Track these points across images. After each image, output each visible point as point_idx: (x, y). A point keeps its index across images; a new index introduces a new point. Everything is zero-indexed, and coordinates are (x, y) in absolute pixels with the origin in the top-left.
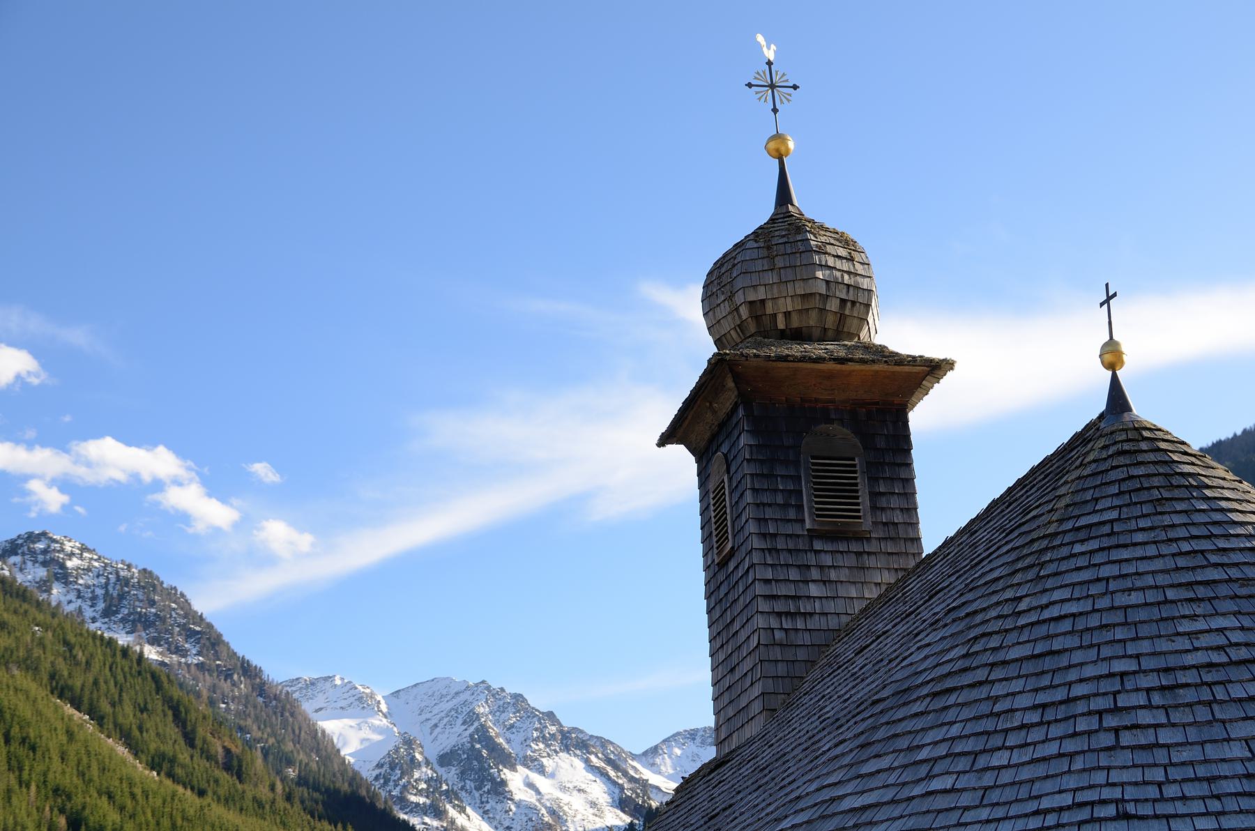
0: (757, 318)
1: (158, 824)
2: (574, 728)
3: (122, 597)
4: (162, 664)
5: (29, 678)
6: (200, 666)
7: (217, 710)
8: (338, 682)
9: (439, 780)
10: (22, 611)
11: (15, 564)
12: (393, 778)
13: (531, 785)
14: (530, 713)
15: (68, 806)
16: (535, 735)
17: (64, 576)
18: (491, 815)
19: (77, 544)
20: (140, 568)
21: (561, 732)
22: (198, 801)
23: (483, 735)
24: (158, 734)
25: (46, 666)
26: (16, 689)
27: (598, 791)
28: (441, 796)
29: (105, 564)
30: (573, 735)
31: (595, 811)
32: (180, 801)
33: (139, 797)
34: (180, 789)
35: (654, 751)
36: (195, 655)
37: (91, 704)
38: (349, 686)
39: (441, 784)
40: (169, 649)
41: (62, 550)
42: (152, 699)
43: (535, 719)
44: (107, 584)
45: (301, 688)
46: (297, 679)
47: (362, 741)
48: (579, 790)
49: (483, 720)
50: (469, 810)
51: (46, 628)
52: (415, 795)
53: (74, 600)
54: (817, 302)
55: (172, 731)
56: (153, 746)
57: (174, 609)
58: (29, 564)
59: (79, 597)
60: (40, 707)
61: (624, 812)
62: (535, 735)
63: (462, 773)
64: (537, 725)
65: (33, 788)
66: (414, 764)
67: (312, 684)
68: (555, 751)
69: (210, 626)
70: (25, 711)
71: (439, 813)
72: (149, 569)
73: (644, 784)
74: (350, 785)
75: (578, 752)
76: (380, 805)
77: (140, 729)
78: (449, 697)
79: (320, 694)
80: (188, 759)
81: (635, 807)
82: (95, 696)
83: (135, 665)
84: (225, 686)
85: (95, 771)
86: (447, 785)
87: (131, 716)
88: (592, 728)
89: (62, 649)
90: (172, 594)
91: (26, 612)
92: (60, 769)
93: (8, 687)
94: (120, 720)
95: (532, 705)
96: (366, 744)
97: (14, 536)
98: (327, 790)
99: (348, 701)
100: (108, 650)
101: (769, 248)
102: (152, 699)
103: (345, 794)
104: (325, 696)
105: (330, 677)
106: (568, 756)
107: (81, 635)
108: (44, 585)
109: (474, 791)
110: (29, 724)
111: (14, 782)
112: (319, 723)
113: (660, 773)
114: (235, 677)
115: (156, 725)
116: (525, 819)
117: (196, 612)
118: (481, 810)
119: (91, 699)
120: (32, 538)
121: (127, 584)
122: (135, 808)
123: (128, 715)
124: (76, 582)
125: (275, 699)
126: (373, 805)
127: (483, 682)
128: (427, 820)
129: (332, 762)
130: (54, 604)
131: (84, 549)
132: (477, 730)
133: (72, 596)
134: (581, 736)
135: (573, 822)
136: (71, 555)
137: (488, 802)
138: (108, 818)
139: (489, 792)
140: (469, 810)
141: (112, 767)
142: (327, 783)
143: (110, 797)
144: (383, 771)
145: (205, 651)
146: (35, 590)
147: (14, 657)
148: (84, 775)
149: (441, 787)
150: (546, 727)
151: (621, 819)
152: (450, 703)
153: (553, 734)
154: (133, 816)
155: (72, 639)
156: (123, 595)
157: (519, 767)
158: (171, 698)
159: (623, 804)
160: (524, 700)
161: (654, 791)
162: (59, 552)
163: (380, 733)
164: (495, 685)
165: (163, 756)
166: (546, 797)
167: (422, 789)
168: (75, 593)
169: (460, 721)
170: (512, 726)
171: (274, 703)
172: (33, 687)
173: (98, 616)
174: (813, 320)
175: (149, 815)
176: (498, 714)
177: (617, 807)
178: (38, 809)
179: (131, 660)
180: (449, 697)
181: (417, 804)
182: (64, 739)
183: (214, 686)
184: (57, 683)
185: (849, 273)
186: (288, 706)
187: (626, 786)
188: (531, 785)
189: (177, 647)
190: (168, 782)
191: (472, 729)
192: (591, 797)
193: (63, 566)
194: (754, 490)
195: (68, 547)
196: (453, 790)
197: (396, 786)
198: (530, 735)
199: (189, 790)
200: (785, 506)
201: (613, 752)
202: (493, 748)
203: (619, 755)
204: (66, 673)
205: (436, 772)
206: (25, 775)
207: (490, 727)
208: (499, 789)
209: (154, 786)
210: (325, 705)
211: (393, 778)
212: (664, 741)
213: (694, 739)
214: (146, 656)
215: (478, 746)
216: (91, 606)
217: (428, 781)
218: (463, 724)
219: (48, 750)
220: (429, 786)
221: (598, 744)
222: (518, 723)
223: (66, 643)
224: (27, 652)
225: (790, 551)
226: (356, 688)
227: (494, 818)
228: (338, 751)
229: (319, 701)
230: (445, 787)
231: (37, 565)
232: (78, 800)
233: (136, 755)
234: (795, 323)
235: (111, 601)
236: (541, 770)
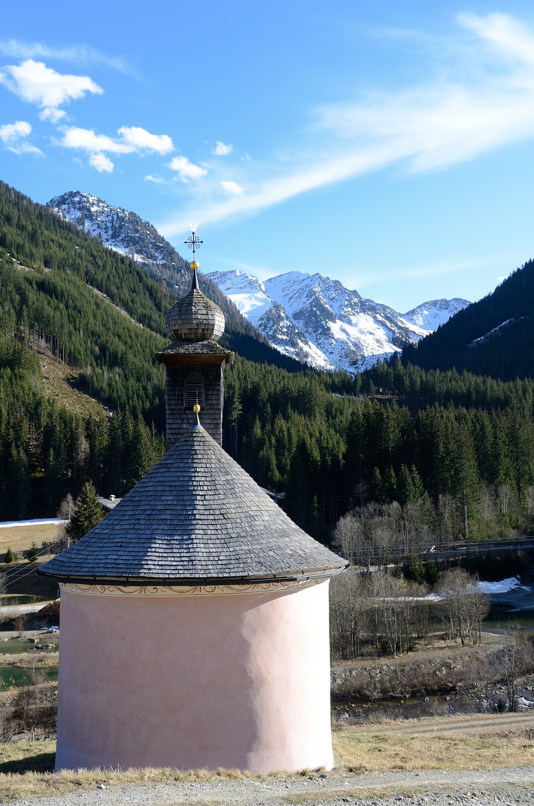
0: (177, 335)
1: (144, 351)
2: (368, 300)
3: (121, 227)
4: (144, 264)
5: (75, 275)
6: (164, 265)
7: (174, 289)
8: (238, 274)
9: (294, 327)
10: (69, 238)
11: (65, 209)
12: (269, 326)
13: (344, 330)
14: (344, 291)
15: (99, 341)
16: (346, 303)
17: (90, 216)
18: (322, 346)
19: (96, 198)
20: (129, 211)
21: (361, 302)
22: (163, 340)
23: (317, 303)
24: (142, 305)
25: (83, 268)
26: (69, 280)
27: (381, 334)
28: (295, 335)
29: (111, 209)
30: (367, 304)
31: (379, 344)
32: (154, 340)
33: (133, 337)
34: (154, 334)
35: (413, 312)
36: (161, 259)
37: (107, 288)
38: (244, 276)
39: (295, 329)
40: (147, 256)
41: (88, 202)
42: (138, 286)
43: (346, 295)
44: (112, 220)
45: (218, 277)
46: (216, 272)
47: (252, 305)
48: (370, 333)
49: (317, 295)
50: (310, 343)
51: (82, 247)
52: (281, 335)
53: (96, 229)
54: (194, 331)
55: (149, 303)
56: (139, 311)
57: (148, 234)
58: (72, 209)
59: (99, 227)
60: (82, 290)
61: (395, 345)
62: (346, 303)
63: (306, 323)
64: (347, 298)
65: (82, 331)
66: (280, 319)
67: (224, 275)
68: (357, 312)
69: (168, 244)
70: (74, 292)
71: (294, 345)
72: (134, 212)
73: (407, 330)
74: (245, 329)
75: (370, 313)
76: (261, 341)
77: (133, 302)
78: (298, 283)
79: (229, 281)
80: (158, 317)
81: (401, 342)
82: (108, 284)
83: (128, 267)
84: (178, 276)
85: (111, 325)
86: (298, 330)
87: (128, 295)
88: (378, 300)
89: (91, 258)
90: (147, 226)
91: (71, 238)
92: (93, 322)
93: (65, 279)
94: (122, 297)
95: (344, 287)
96: (255, 307)
97: (63, 194)
98: (233, 332)
99: (244, 284)
100: (114, 260)
101: (180, 311)
102: (138, 286)
103: (242, 335)
104: (231, 281)
105: (233, 271)
106: (364, 315)
107: (99, 251)
108: (80, 221)
109: (313, 333)
110: (76, 299)
111: (72, 328)
112: (228, 296)
113: (416, 324)
114: (183, 271)
115: (141, 300)
116: (341, 348)
117: (160, 236)
118: (317, 343)
119: (107, 285)
120: (72, 195)
121: (123, 221)
122: (132, 343)
123: (126, 294)
124: (97, 219)
125: (204, 283)
126: (257, 341)
127: (317, 274)
128: (287, 348)
129: (235, 317)
130: (86, 231)
131: (99, 201)
132: (314, 300)
133: (95, 227)
134: (371, 304)
135: (367, 350)
136: (93, 204)
137: (320, 339)
138: (119, 348)
139: (321, 334)
140: (310, 343)
141: (119, 322)
142: (233, 328)
143: (119, 337)
144: (263, 322)
145: (166, 257)
146: (76, 224)
147: (67, 263)
148: (105, 326)
149: (295, 331)
150: (352, 299)
151: (393, 349)
152: (299, 285)
153: (356, 303)
154: (131, 347)
155: (96, 254)
156: (121, 226)
157: (337, 321)
158: (148, 285)
159: (394, 341)
160: (340, 284)
161: (412, 334)
162: (86, 202)
163: (262, 302)
164: (324, 276)
165: (145, 316)
166: (352, 337)
167: (285, 332)
168: (97, 225)
169: (305, 295)
170: (333, 298)
171: (204, 285)
172: (77, 279)
173: (109, 238)
174: (193, 336)
175: (139, 348)
176: (325, 291)
177: (391, 343)
178: (85, 342)
179: (126, 265)
180: (298, 283)
181: (282, 340)
182: (94, 307)
183: (172, 276)
184: (89, 277)
185: (206, 319)
186: (211, 287)
187: (396, 331)
188: (344, 330)
189: (151, 255)
190: (148, 330)
191: (311, 300)
192: (377, 337)
193: (89, 210)
194: (168, 395)
195: (91, 199)
196: (301, 332)
197: (270, 330)
198: (343, 303)
199: (159, 334)
200: (178, 399)
201: (390, 313)
202: (323, 310)
203: (393, 314)
204: (93, 272)
205: (292, 323)
206: (77, 326)
207: (321, 299)
208: (326, 332)
209: (140, 332)
210: (231, 286)
211: (269, 326)
212: (419, 307)
213: (435, 306)
214: (135, 260)
215: (315, 309)
216: (106, 233)
217: (288, 327)
218: (306, 297)
219: (87, 313)
220: (288, 330)
221: (381, 308)
222: (337, 297)
223: (92, 255)
224: (73, 261)
225: (178, 414)
226: (248, 277)
227: (323, 347)
228: (239, 311)
229: (228, 284)
230: (297, 331)
231: (76, 210)
232: (104, 338)
233: (131, 316)
234: (188, 337)
235: (115, 230)
236: (350, 322)
